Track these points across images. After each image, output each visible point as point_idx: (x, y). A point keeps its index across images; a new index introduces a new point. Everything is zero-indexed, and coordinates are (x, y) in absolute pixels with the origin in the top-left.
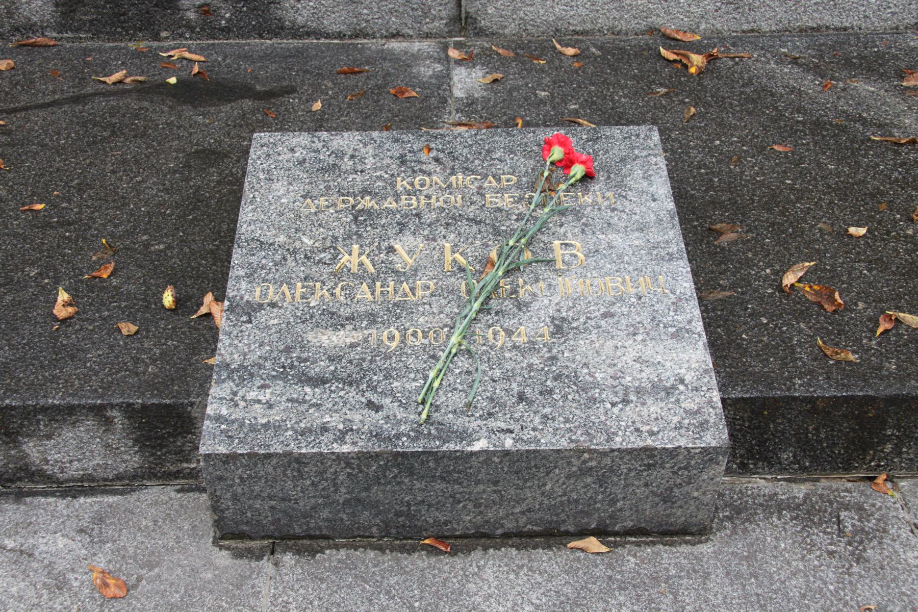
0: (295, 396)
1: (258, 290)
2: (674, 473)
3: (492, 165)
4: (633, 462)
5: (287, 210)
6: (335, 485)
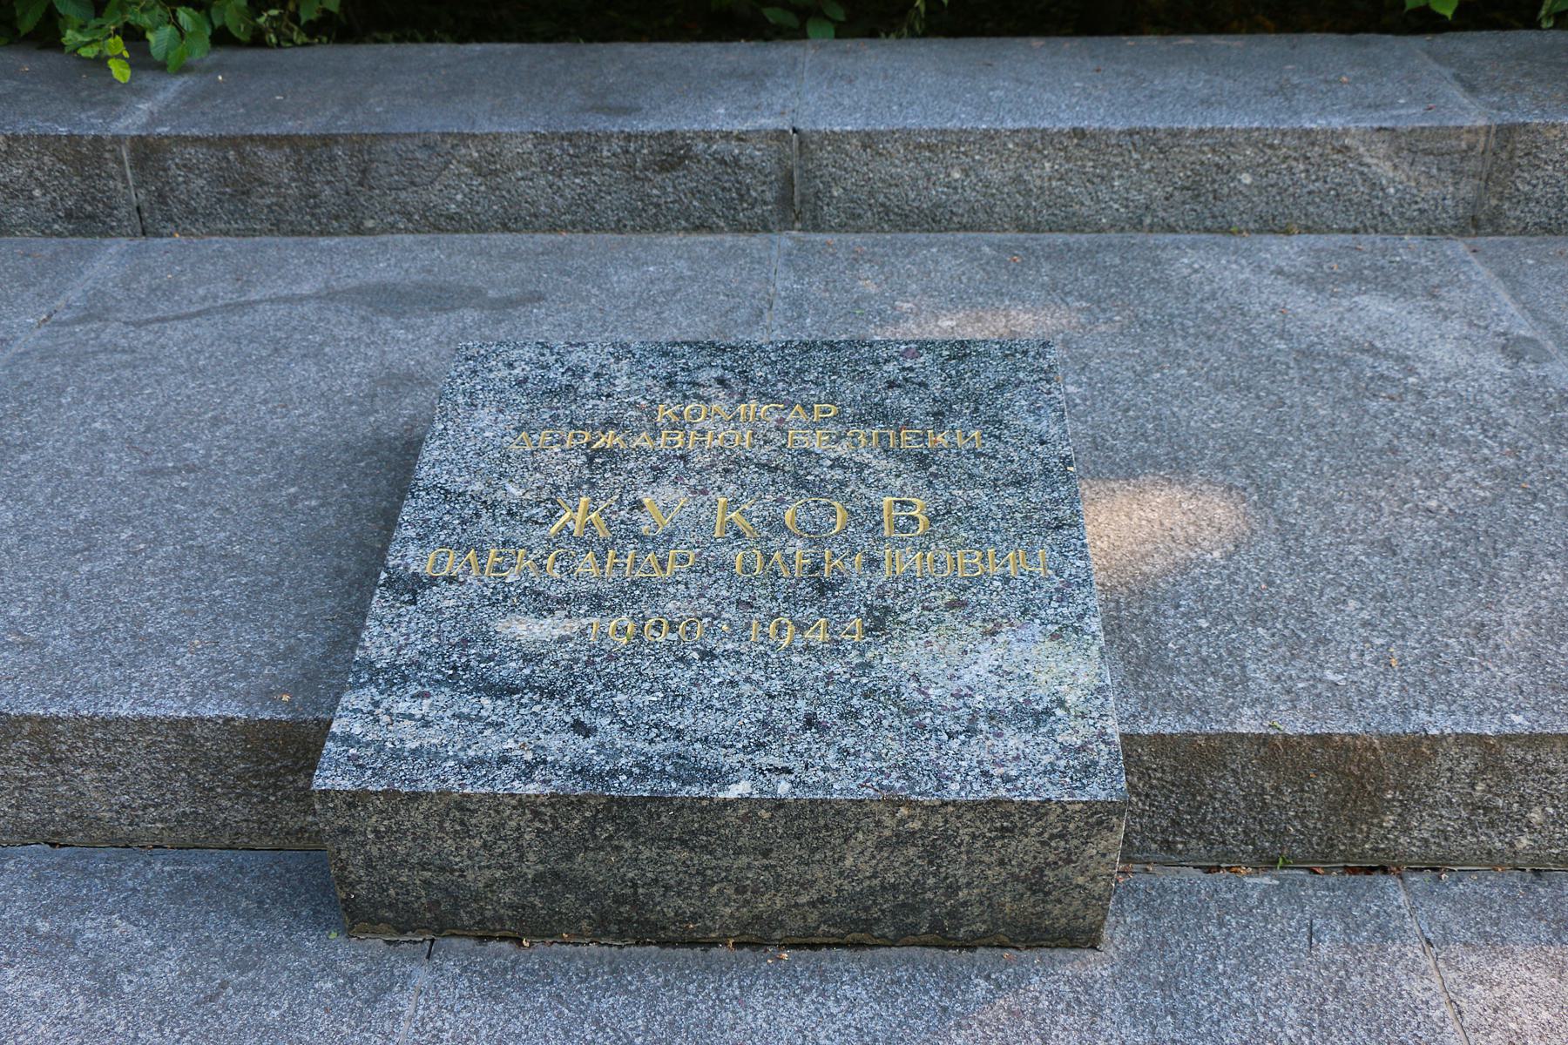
0: (465, 710)
2: (1043, 843)
4: (978, 823)
6: (519, 848)
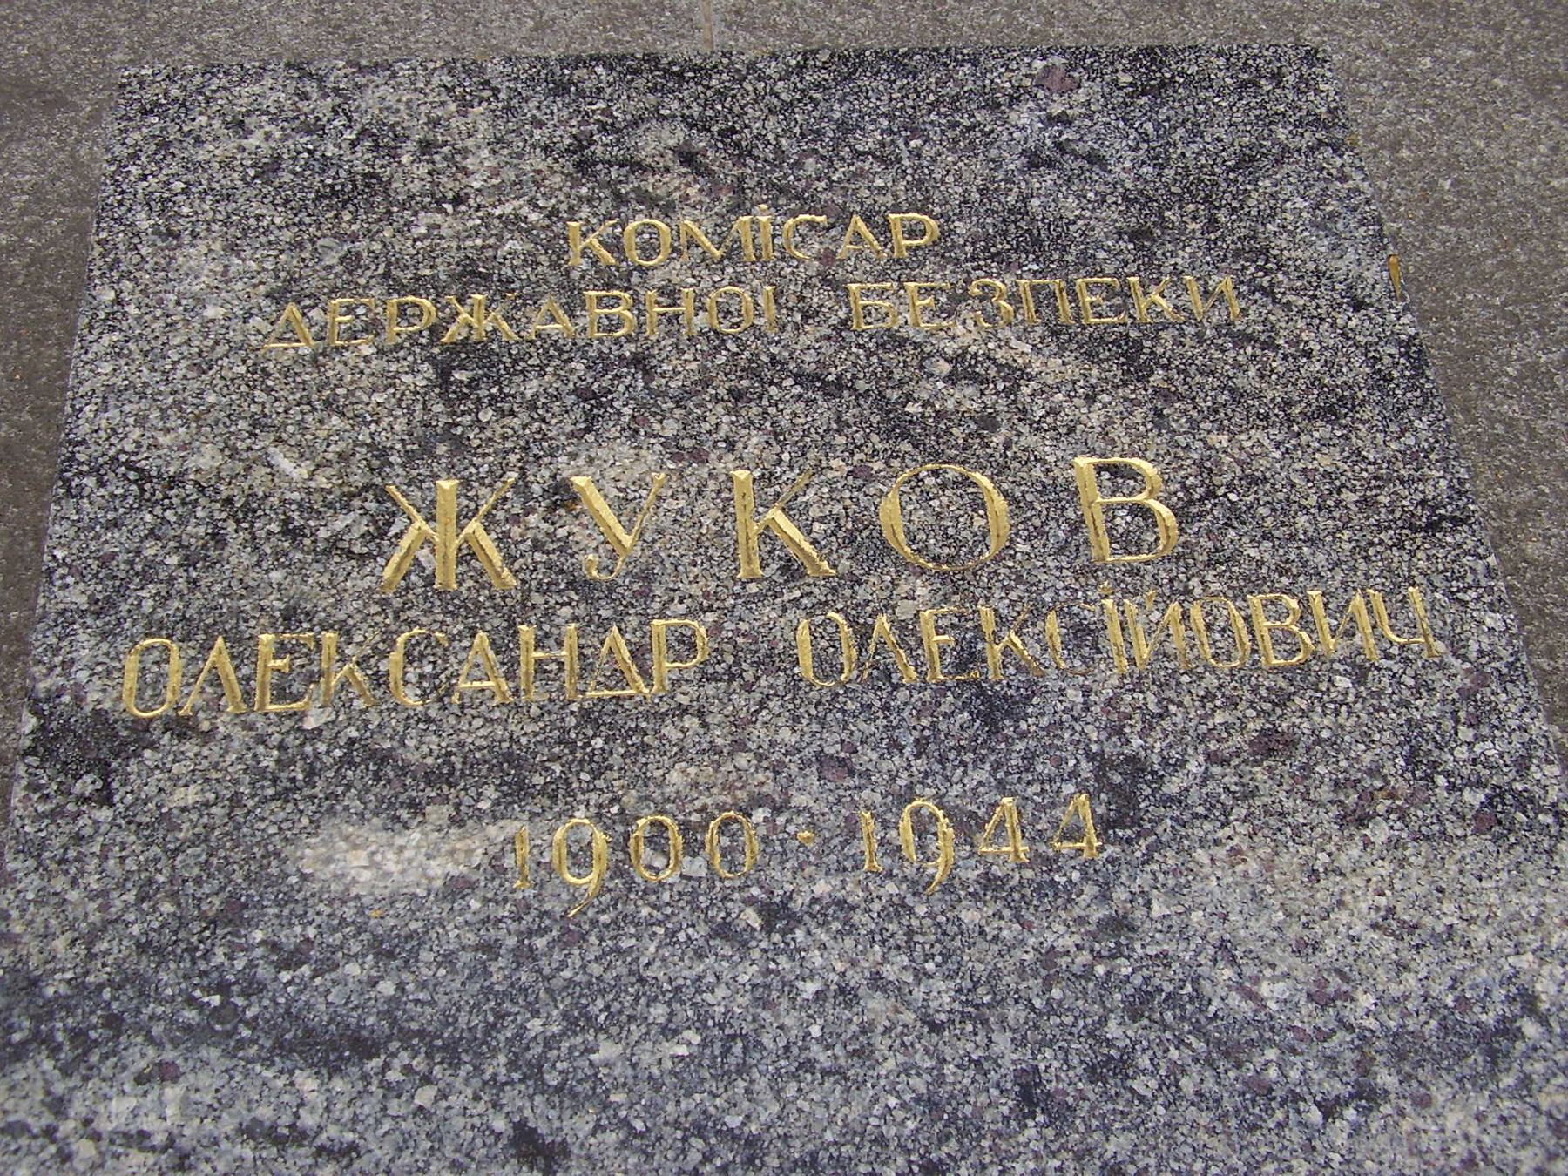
0: (265, 1113)
1: (132, 663)
3: (861, 174)
5: (222, 349)
